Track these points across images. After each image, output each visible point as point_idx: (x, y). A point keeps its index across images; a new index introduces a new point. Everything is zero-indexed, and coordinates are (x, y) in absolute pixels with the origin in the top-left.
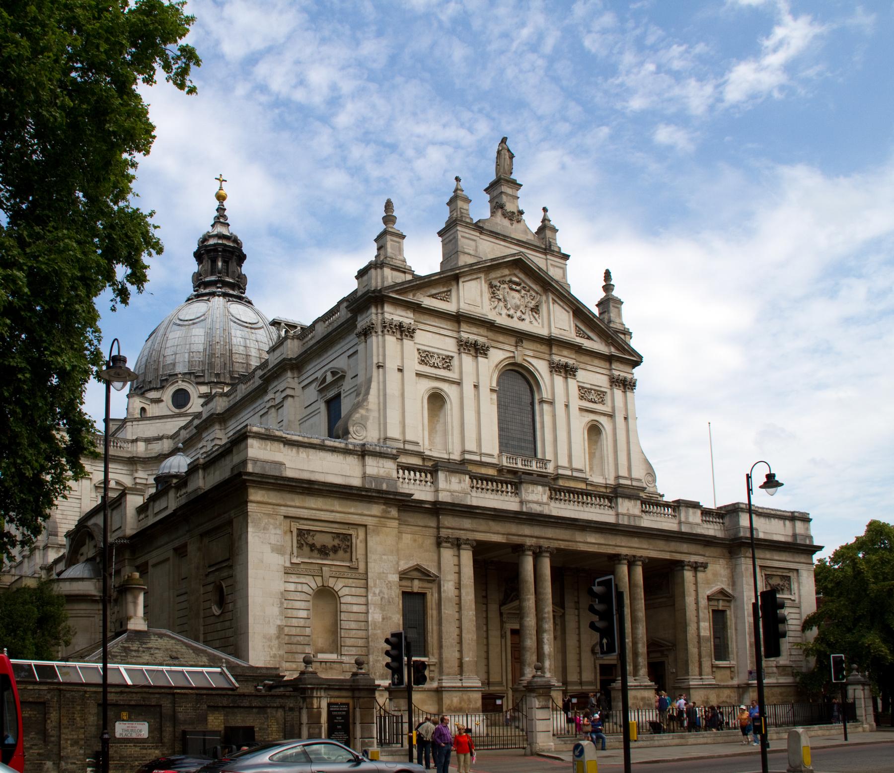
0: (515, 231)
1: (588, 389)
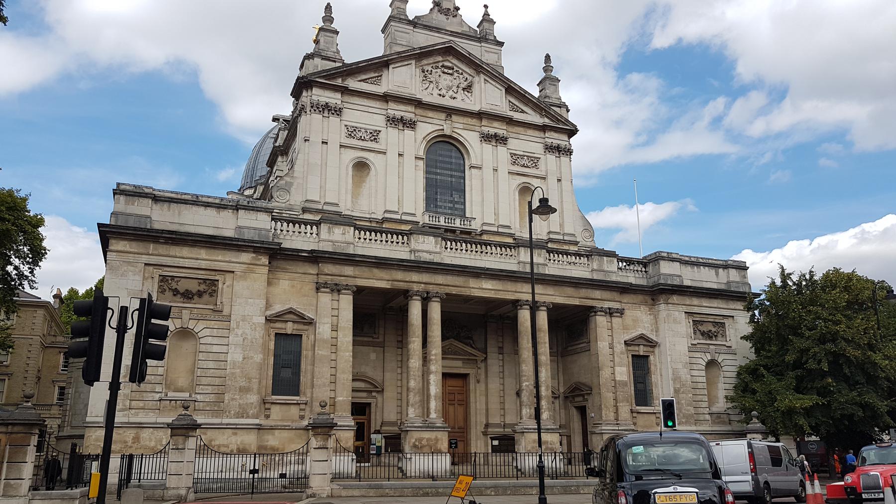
0: (450, 24)
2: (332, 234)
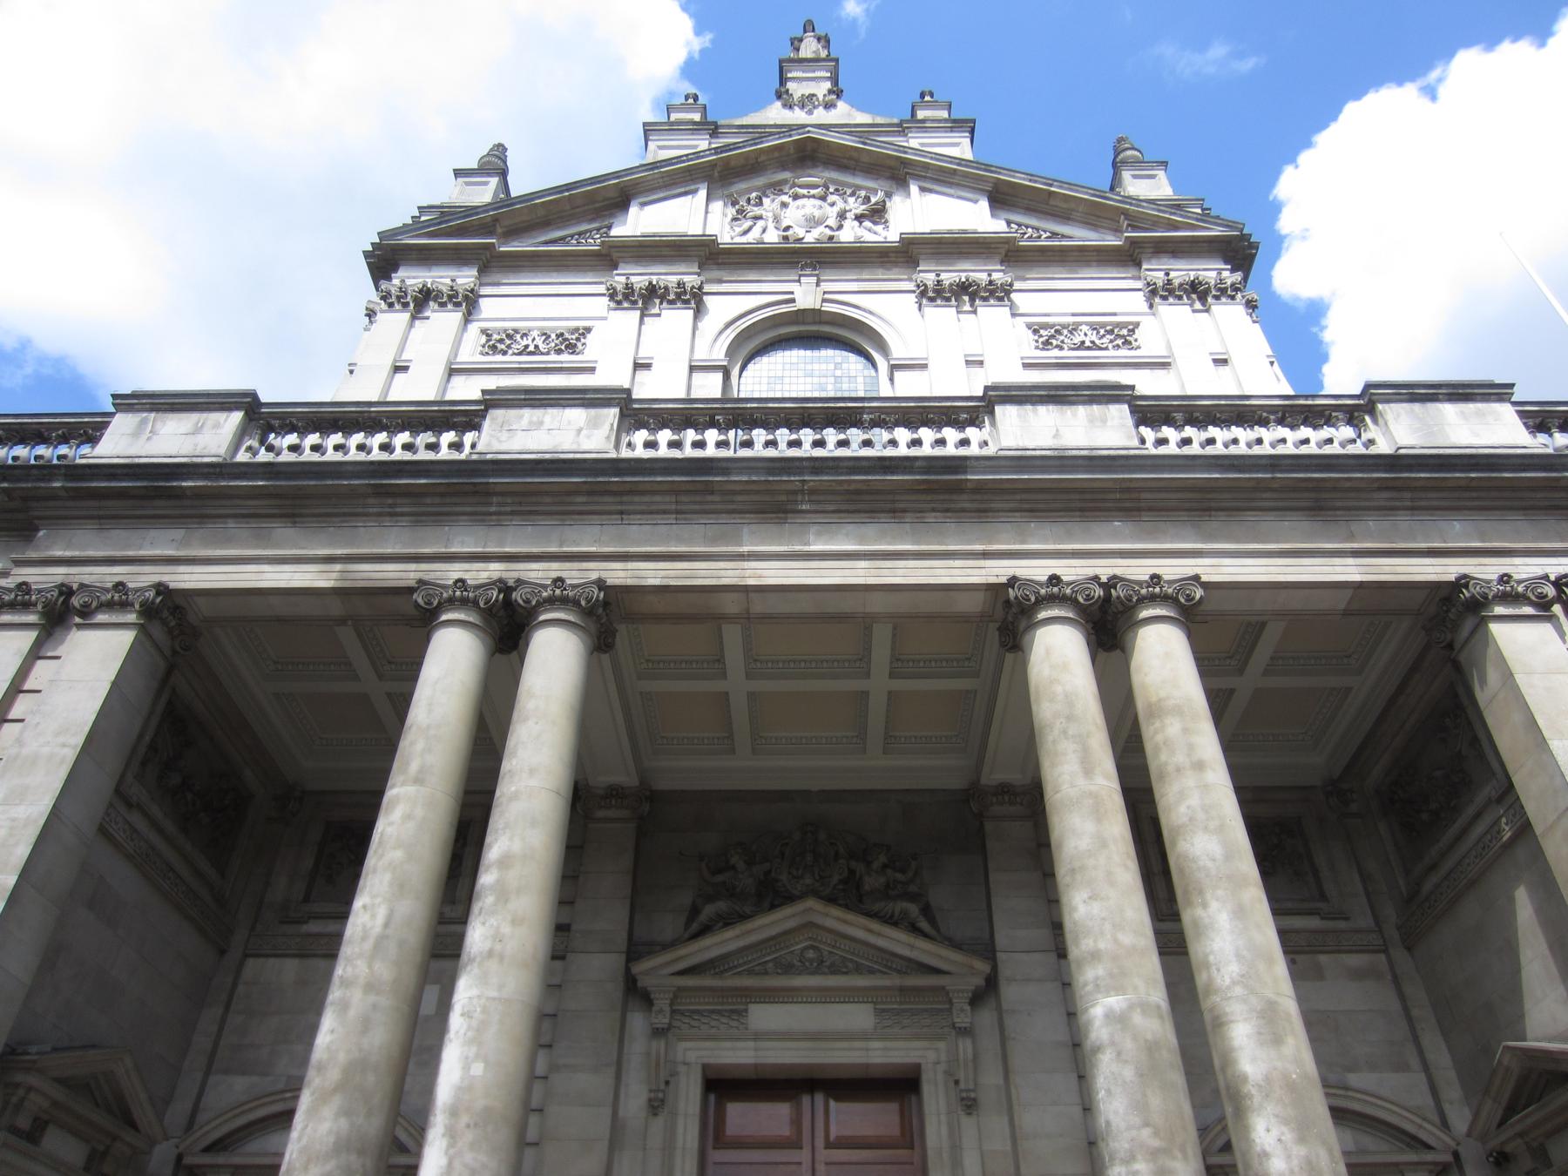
1: (1064, 326)
2: (147, 434)
